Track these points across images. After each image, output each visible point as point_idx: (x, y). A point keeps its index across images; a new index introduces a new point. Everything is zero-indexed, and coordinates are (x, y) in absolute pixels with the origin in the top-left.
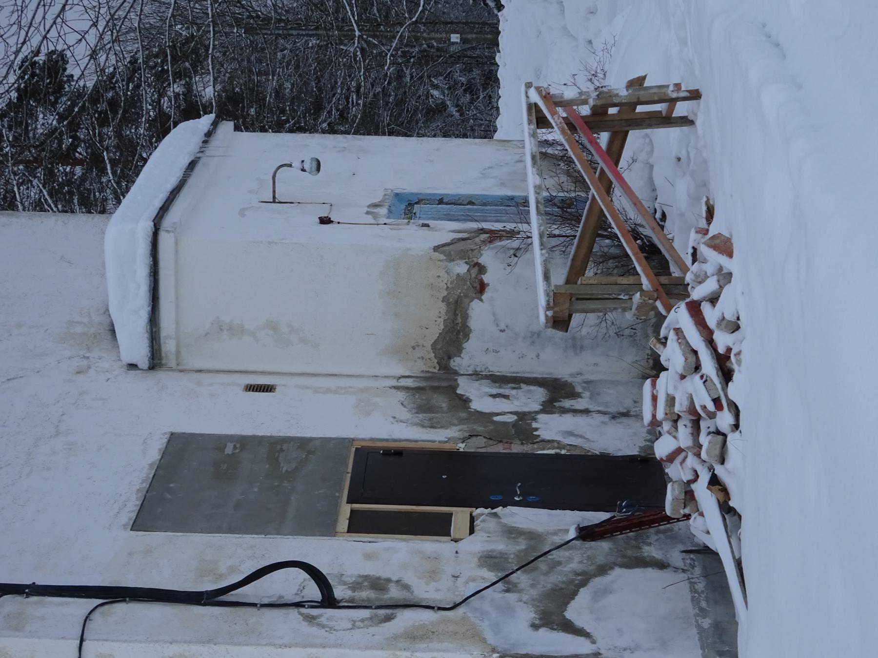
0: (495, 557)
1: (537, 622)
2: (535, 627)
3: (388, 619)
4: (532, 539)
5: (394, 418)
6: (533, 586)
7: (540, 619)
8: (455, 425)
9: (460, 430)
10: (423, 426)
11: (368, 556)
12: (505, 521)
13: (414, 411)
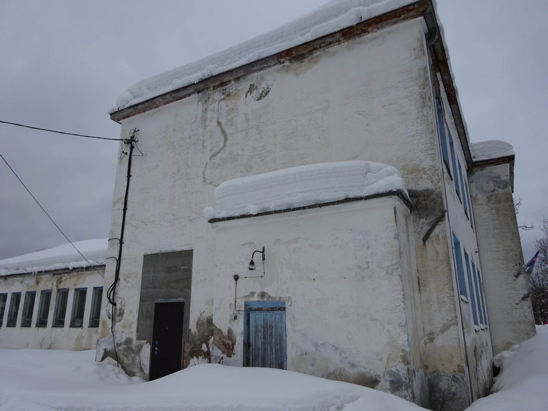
0: (130, 341)
1: (106, 350)
2: (105, 350)
3: (109, 318)
4: (137, 351)
5: (204, 312)
6: (119, 350)
7: (107, 351)
8: (198, 331)
9: (195, 333)
10: (198, 322)
11: (131, 312)
12: (145, 344)
13: (209, 318)
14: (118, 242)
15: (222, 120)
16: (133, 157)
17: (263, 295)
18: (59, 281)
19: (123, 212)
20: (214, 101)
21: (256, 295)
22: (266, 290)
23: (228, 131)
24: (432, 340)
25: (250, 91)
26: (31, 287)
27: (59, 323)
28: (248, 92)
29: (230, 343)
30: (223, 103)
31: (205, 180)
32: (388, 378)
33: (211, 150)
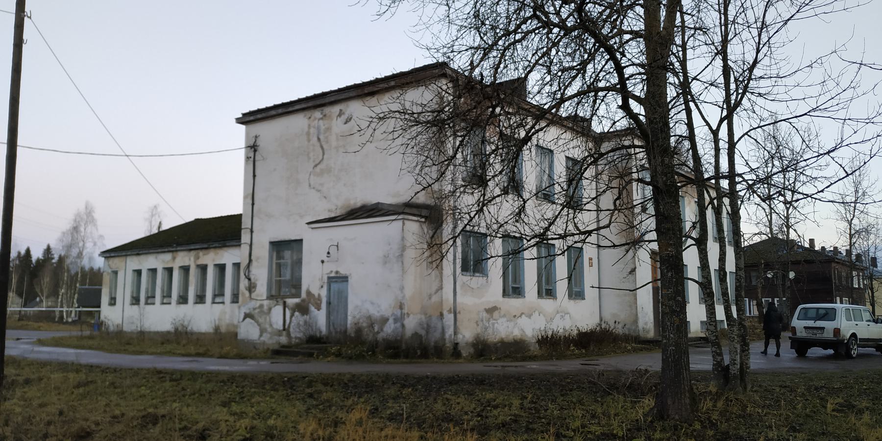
3: (246, 289)
14: (249, 231)
15: (321, 137)
16: (257, 163)
17: (337, 272)
18: (197, 258)
19: (251, 206)
20: (315, 119)
21: (333, 273)
22: (339, 270)
23: (325, 147)
24: (430, 298)
25: (340, 115)
26: (168, 262)
27: (200, 299)
28: (338, 116)
29: (319, 302)
30: (321, 121)
31: (310, 186)
32: (393, 317)
33: (314, 161)
